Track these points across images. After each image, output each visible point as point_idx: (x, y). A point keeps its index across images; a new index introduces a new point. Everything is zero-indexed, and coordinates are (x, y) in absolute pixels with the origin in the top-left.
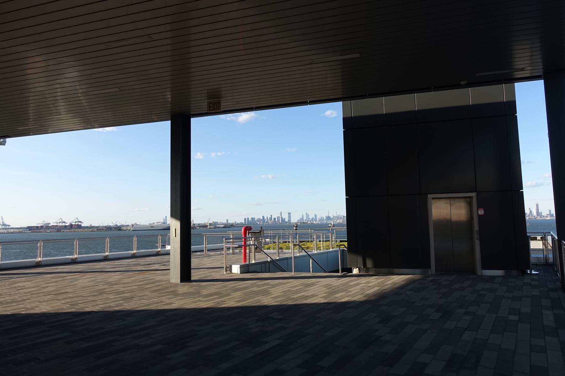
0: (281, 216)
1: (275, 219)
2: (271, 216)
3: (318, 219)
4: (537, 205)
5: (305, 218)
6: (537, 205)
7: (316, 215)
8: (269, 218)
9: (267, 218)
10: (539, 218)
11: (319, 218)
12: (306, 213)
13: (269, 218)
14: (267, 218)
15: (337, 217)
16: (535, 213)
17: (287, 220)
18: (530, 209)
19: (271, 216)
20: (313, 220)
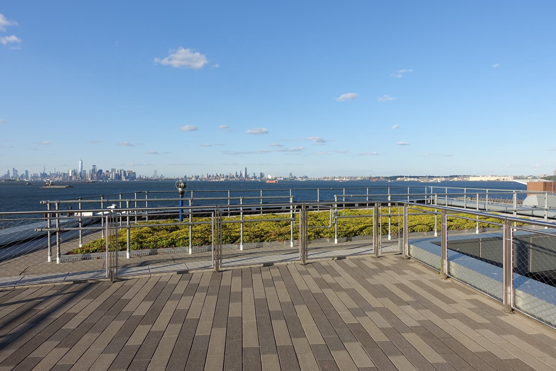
3: (30, 176)
4: (246, 169)
5: (11, 174)
6: (246, 169)
7: (27, 172)
10: (246, 180)
11: (31, 175)
12: (14, 169)
15: (55, 174)
16: (244, 176)
18: (240, 172)
20: (23, 178)
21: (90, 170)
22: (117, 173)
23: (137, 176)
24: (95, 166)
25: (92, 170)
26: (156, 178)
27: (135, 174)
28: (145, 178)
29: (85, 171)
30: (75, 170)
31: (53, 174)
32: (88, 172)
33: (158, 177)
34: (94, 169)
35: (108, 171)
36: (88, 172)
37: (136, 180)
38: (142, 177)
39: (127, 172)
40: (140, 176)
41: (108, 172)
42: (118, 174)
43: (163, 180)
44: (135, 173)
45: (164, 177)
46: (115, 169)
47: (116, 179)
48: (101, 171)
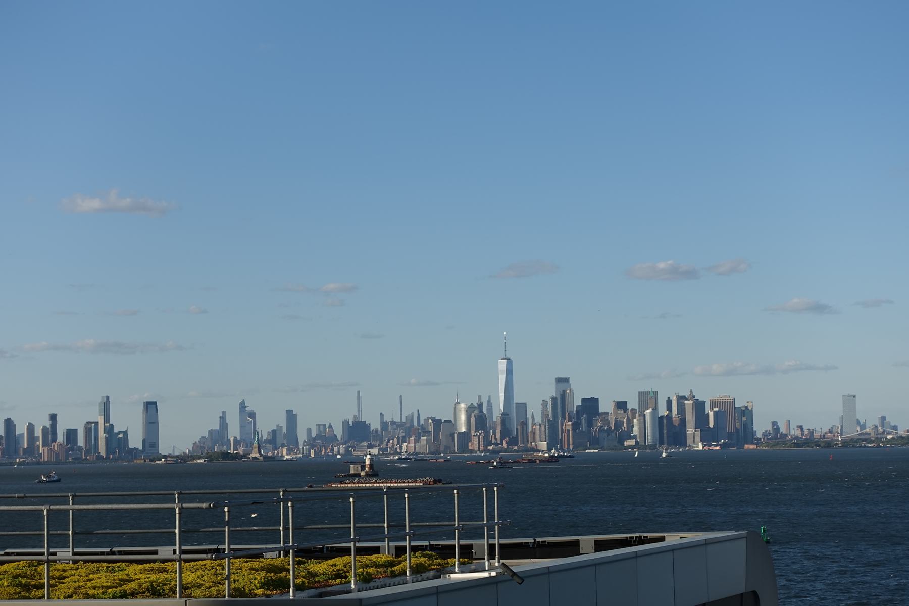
0: (107, 419)
1: (71, 435)
2: (53, 417)
3: (302, 437)
5: (234, 432)
7: (291, 417)
8: (38, 433)
9: (31, 428)
12: (243, 406)
13: (38, 433)
14: (31, 428)
15: (400, 425)
17: (135, 442)
19: (53, 417)
20: (279, 441)
21: (545, 404)
22: (663, 411)
23: (761, 427)
24: (566, 380)
25: (554, 400)
26: (852, 432)
27: (751, 410)
28: (798, 433)
29: (525, 405)
30: (480, 406)
31: (393, 423)
32: (535, 413)
33: (863, 427)
34: (563, 395)
35: (622, 405)
36: (535, 413)
37: (752, 447)
38: (783, 430)
39: (713, 404)
40: (774, 423)
41: (625, 410)
42: (669, 417)
43: (888, 441)
44: (746, 412)
45: (895, 428)
46: (656, 393)
47: (661, 443)
48: (591, 405)
